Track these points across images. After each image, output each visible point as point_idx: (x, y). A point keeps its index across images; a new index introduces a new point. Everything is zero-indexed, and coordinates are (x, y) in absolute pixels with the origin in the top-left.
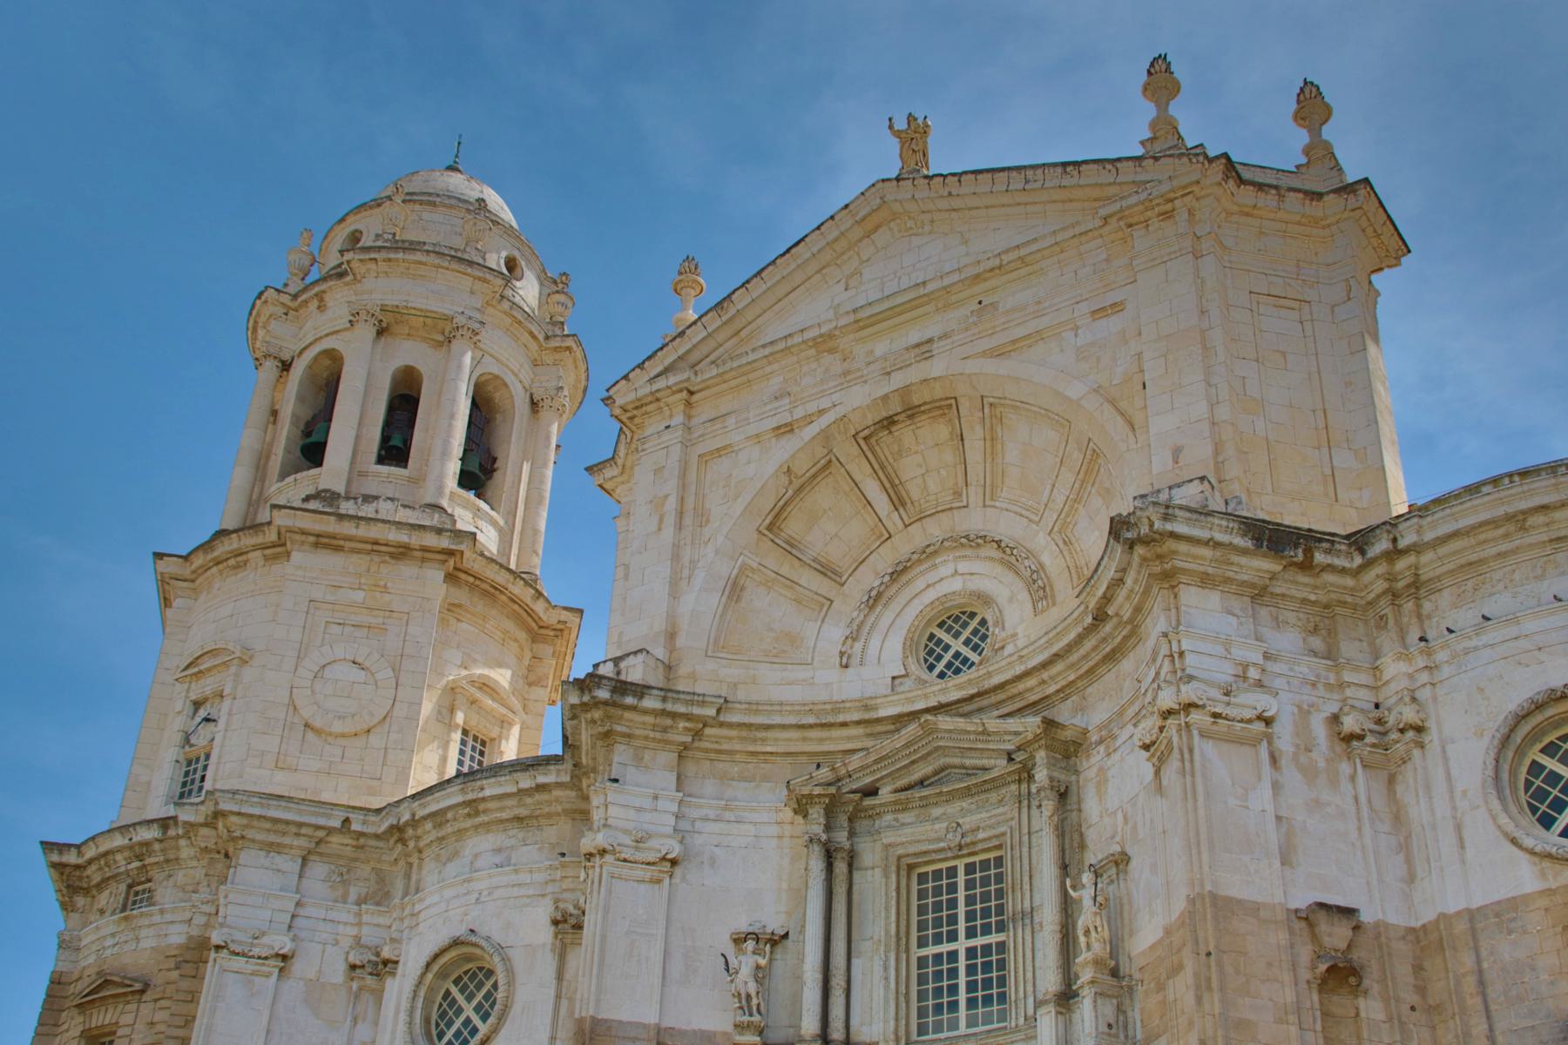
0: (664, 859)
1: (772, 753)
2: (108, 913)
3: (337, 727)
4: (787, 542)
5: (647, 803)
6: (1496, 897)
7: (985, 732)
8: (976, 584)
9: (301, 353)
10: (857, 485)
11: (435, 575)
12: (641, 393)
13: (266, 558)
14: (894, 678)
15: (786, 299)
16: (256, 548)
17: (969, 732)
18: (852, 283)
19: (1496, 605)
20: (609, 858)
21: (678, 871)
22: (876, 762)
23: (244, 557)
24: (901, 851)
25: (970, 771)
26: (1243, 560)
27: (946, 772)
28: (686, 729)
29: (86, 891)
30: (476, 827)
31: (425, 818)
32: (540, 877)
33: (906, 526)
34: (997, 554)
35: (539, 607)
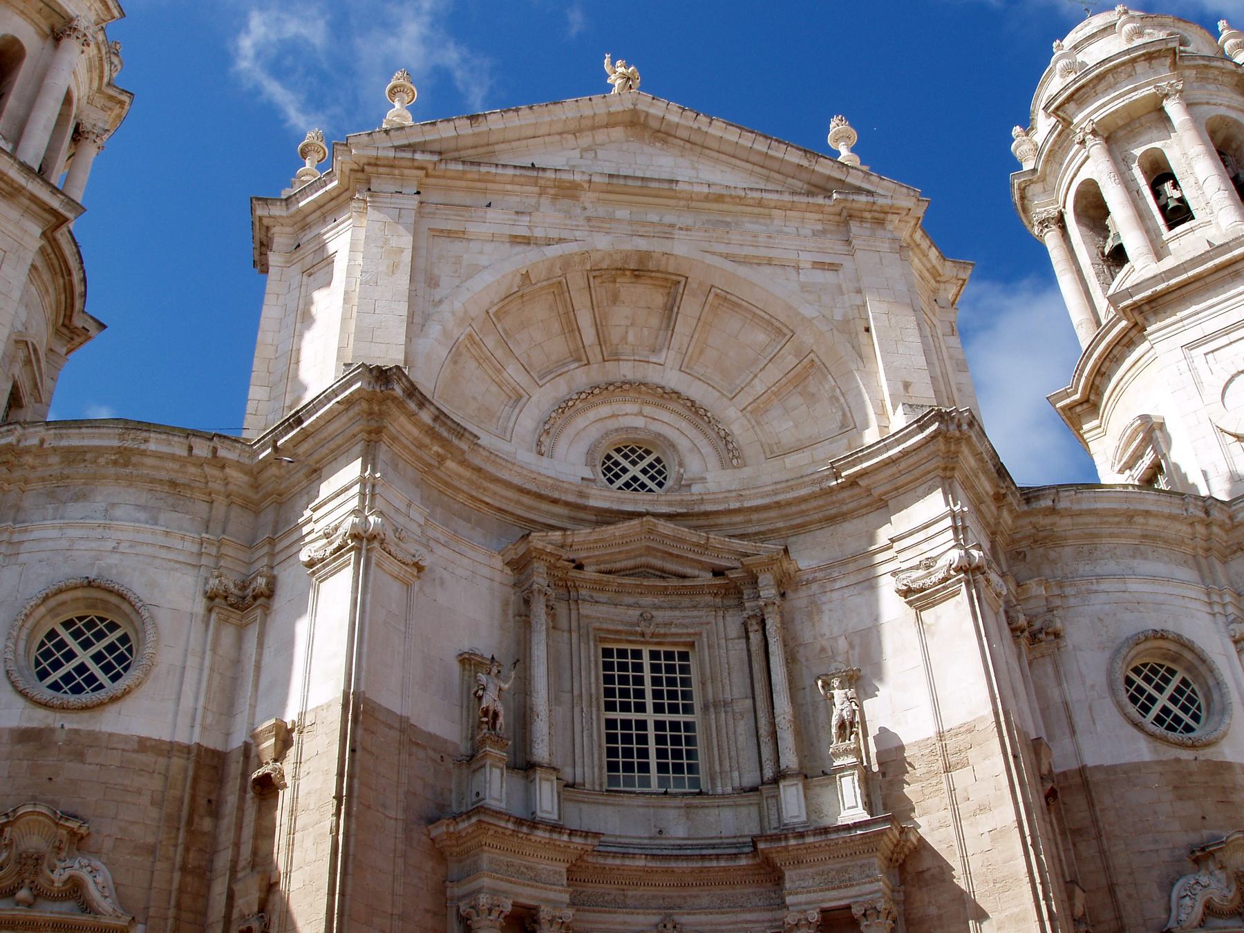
4: (505, 330)
5: (403, 508)
6: (1122, 761)
7: (706, 547)
8: (656, 427)
11: (37, 231)
12: (381, 153)
14: (583, 479)
15: (525, 142)
17: (683, 541)
18: (590, 155)
20: (376, 544)
21: (421, 574)
22: (595, 541)
24: (597, 625)
25: (663, 574)
26: (983, 478)
31: (54, 449)
33: (604, 360)
34: (685, 412)
35: (78, 304)
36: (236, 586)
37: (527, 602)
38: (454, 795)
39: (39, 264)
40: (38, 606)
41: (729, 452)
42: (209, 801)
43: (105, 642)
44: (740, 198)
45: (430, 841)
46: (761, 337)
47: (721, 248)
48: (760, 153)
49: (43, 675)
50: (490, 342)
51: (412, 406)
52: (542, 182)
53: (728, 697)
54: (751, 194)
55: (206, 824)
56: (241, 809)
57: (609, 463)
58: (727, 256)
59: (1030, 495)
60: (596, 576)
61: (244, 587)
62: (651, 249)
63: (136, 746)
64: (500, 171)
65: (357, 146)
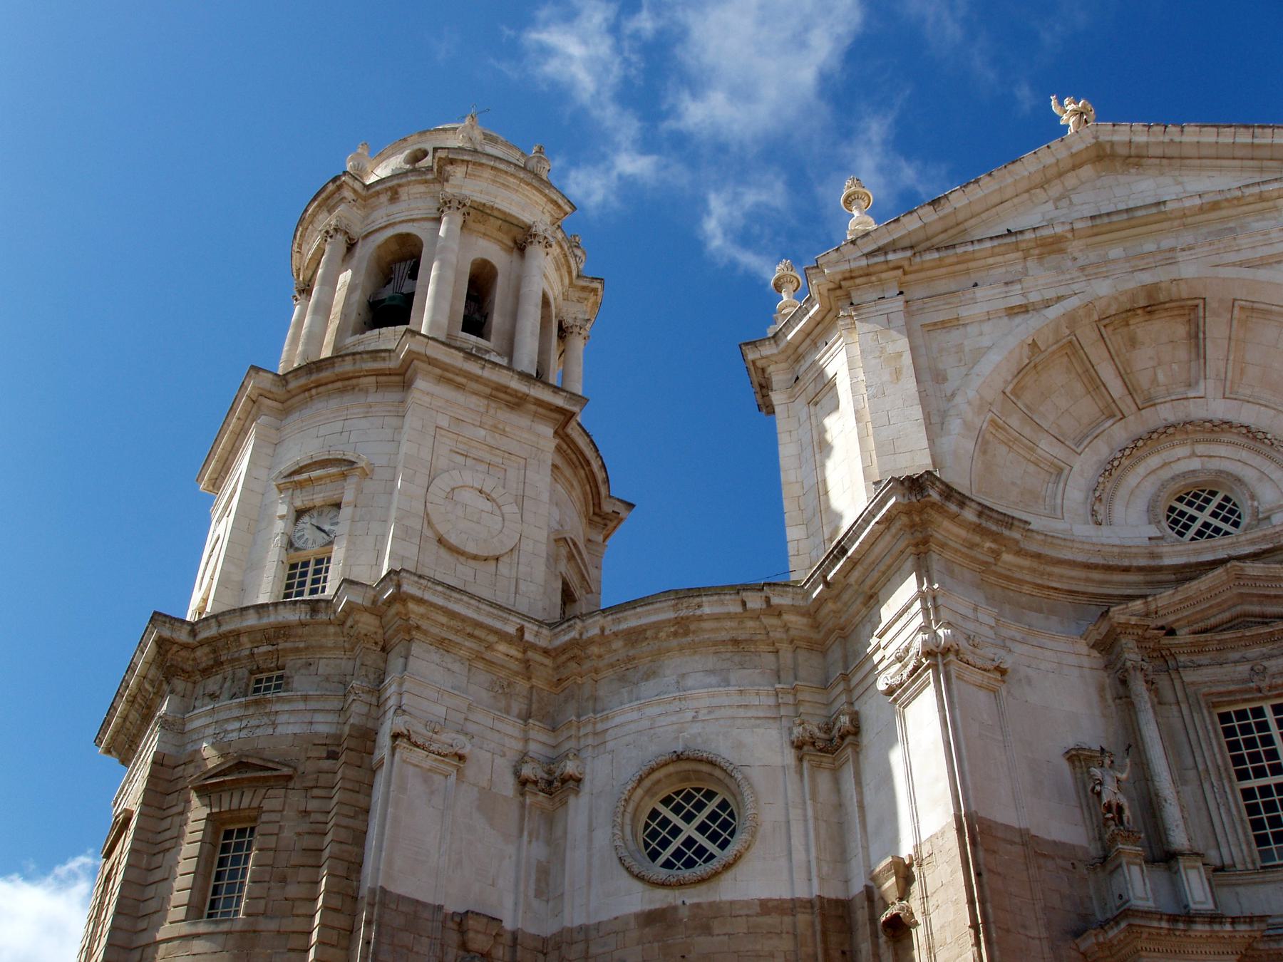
1: (1056, 589)
2: (226, 695)
3: (471, 548)
4: (1027, 406)
5: (970, 613)
8: (1215, 465)
9: (366, 237)
10: (1093, 367)
11: (549, 431)
12: (854, 265)
13: (379, 386)
15: (994, 210)
18: (1064, 203)
20: (951, 657)
21: (1006, 678)
22: (1181, 602)
24: (1206, 690)
27: (1240, 620)
28: (990, 548)
30: (681, 649)
31: (616, 634)
33: (1139, 409)
34: (1242, 440)
35: (603, 490)
36: (820, 729)
37: (1124, 682)
38: (1095, 902)
39: (559, 462)
40: (634, 789)
42: (843, 953)
43: (706, 812)
44: (1238, 199)
45: (1081, 956)
47: (1232, 257)
48: (1244, 145)
49: (654, 855)
50: (1015, 422)
51: (953, 508)
52: (1023, 246)
54: (1248, 191)
57: (1174, 516)
58: (1241, 264)
60: (1190, 638)
61: (828, 730)
62: (1156, 280)
63: (758, 910)
64: (977, 247)
65: (828, 264)
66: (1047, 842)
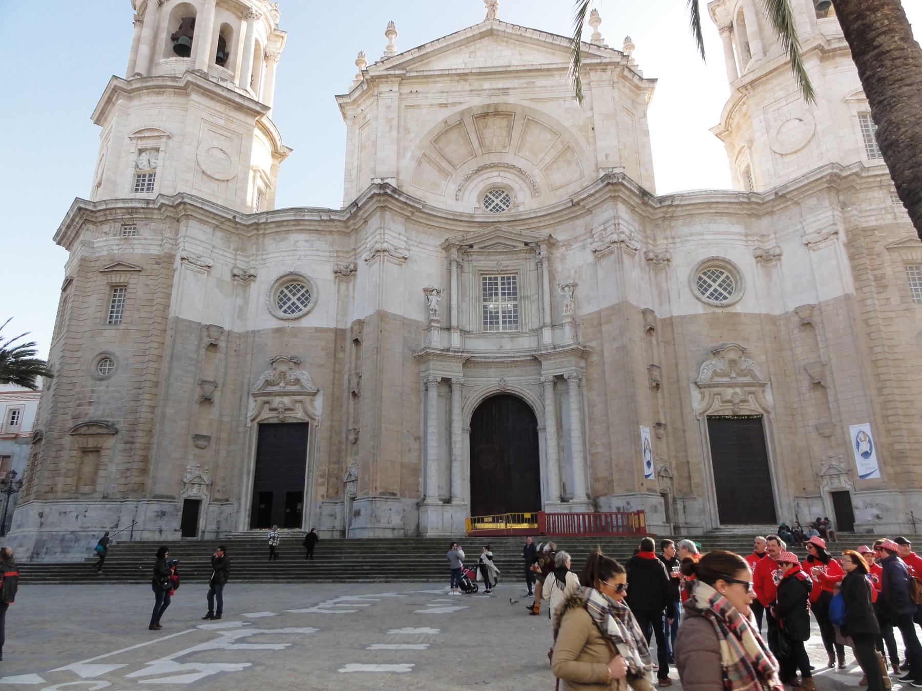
0: (403, 257)
3: (216, 176)
7: (520, 235)
13: (175, 93)
16: (170, 87)
17: (512, 233)
19: (696, 228)
20: (386, 253)
23: (164, 90)
29: (94, 223)
31: (272, 222)
32: (328, 254)
41: (534, 190)
46: (549, 136)
47: (531, 97)
48: (549, 43)
49: (281, 307)
53: (529, 293)
55: (341, 355)
56: (351, 350)
58: (532, 100)
59: (662, 200)
62: (498, 102)
66: (409, 319)
